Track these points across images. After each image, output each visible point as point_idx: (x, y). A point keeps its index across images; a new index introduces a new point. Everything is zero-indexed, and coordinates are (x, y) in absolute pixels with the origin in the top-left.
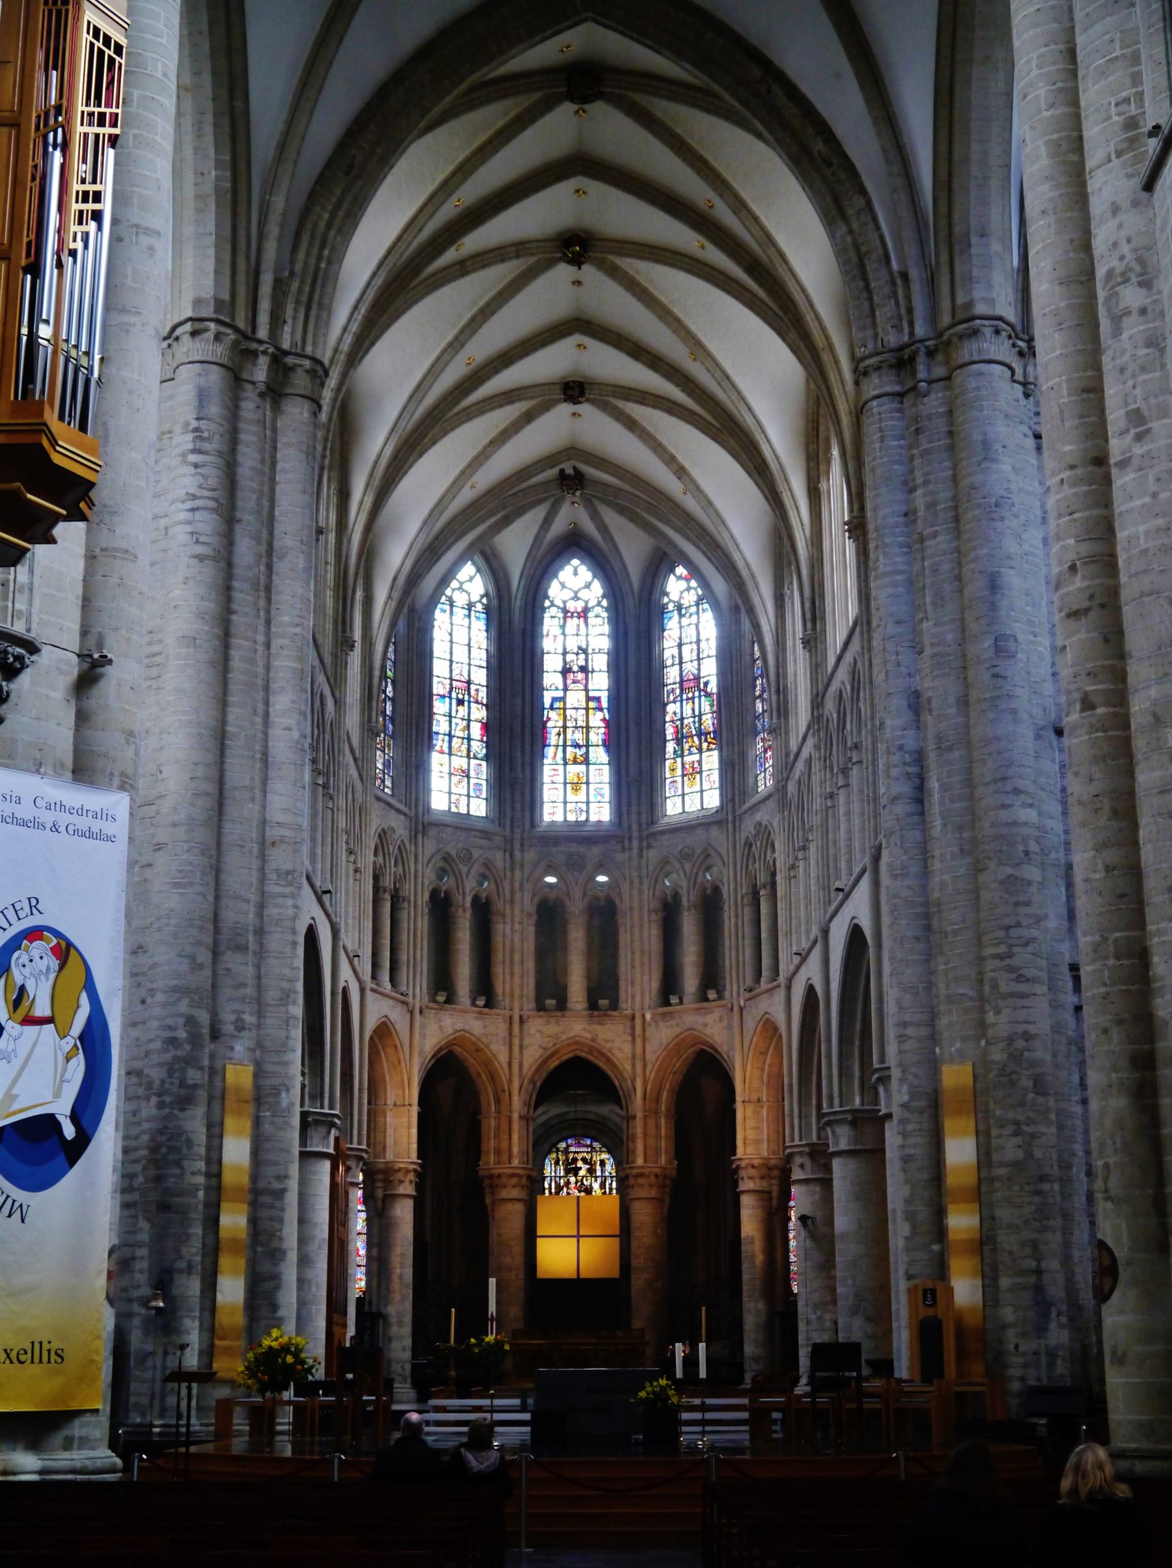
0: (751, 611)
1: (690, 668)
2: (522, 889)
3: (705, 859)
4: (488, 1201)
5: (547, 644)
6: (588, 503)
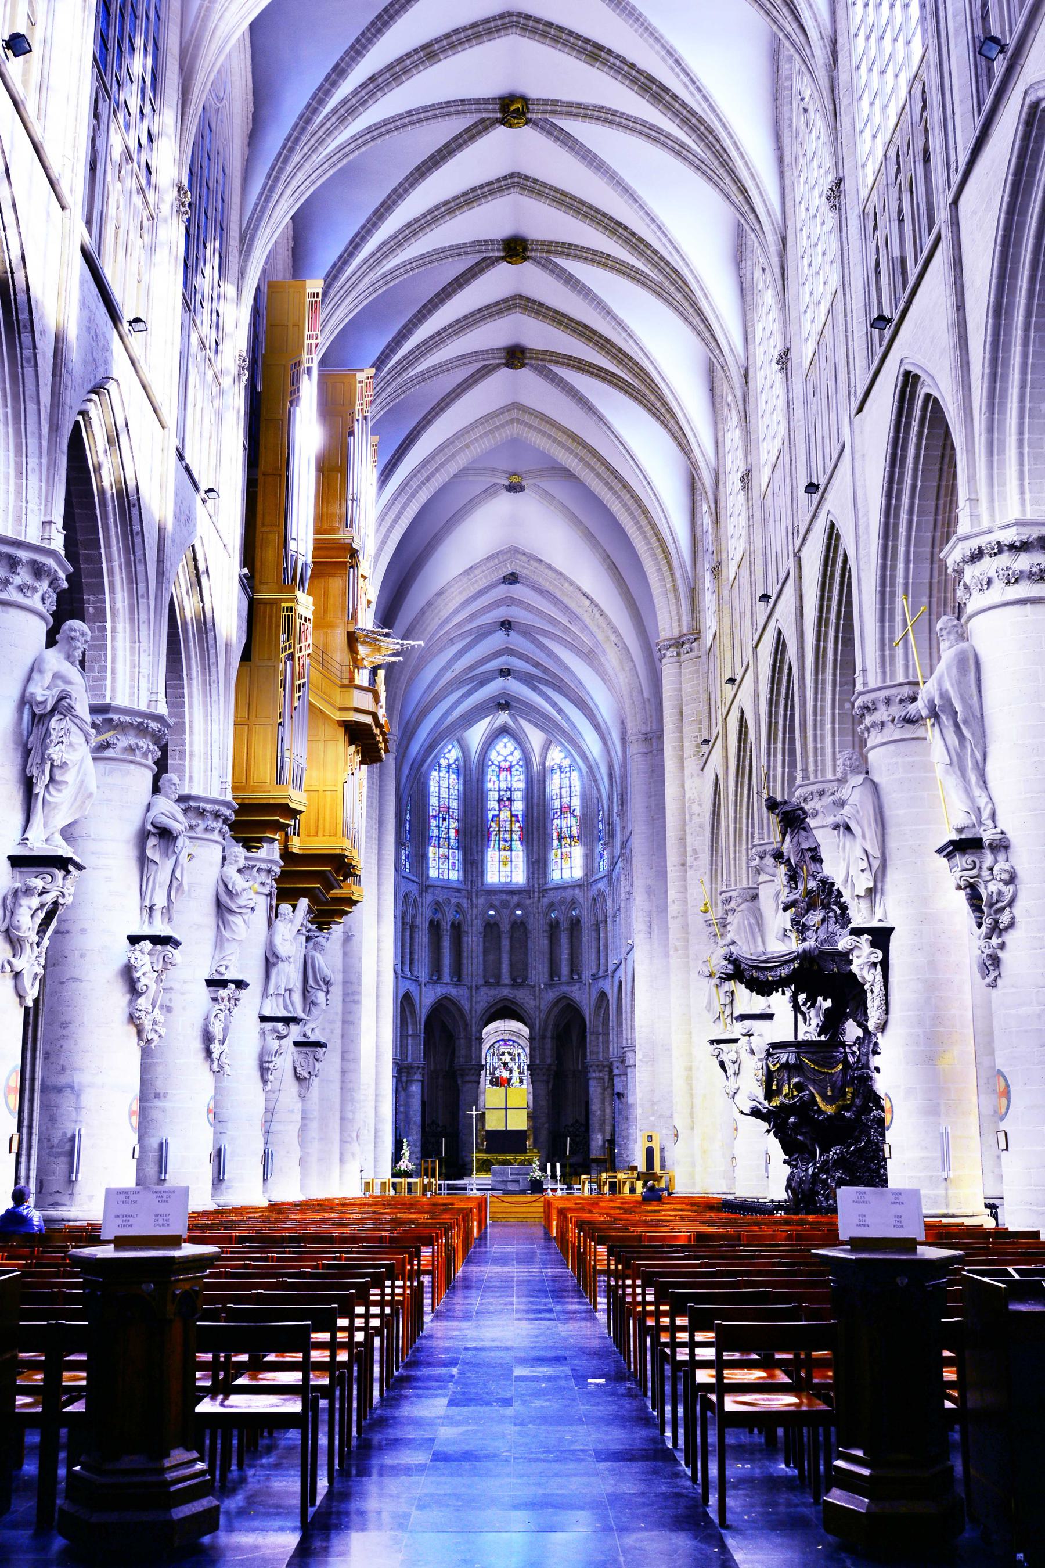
0: (595, 781)
1: (566, 801)
2: (476, 918)
3: (573, 904)
4: (459, 1082)
5: (490, 785)
6: (511, 716)
